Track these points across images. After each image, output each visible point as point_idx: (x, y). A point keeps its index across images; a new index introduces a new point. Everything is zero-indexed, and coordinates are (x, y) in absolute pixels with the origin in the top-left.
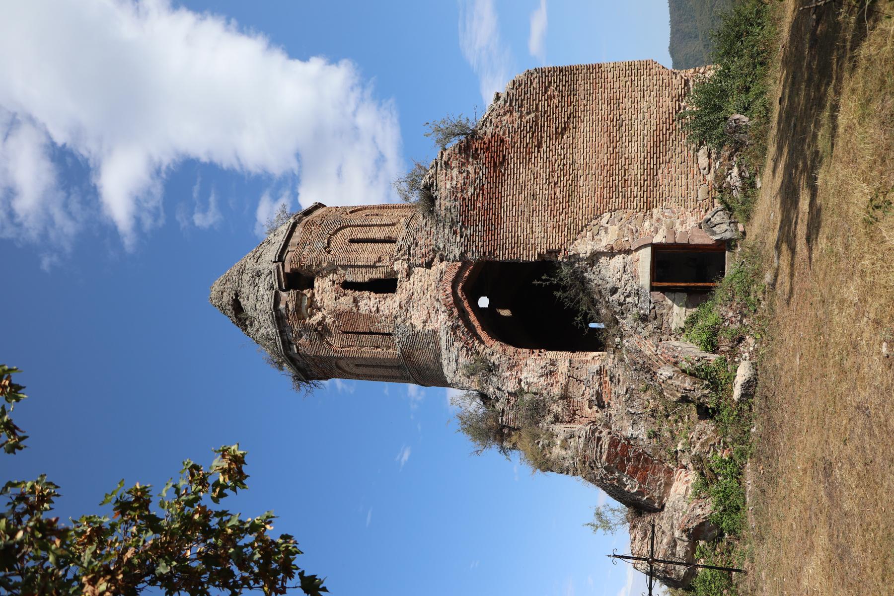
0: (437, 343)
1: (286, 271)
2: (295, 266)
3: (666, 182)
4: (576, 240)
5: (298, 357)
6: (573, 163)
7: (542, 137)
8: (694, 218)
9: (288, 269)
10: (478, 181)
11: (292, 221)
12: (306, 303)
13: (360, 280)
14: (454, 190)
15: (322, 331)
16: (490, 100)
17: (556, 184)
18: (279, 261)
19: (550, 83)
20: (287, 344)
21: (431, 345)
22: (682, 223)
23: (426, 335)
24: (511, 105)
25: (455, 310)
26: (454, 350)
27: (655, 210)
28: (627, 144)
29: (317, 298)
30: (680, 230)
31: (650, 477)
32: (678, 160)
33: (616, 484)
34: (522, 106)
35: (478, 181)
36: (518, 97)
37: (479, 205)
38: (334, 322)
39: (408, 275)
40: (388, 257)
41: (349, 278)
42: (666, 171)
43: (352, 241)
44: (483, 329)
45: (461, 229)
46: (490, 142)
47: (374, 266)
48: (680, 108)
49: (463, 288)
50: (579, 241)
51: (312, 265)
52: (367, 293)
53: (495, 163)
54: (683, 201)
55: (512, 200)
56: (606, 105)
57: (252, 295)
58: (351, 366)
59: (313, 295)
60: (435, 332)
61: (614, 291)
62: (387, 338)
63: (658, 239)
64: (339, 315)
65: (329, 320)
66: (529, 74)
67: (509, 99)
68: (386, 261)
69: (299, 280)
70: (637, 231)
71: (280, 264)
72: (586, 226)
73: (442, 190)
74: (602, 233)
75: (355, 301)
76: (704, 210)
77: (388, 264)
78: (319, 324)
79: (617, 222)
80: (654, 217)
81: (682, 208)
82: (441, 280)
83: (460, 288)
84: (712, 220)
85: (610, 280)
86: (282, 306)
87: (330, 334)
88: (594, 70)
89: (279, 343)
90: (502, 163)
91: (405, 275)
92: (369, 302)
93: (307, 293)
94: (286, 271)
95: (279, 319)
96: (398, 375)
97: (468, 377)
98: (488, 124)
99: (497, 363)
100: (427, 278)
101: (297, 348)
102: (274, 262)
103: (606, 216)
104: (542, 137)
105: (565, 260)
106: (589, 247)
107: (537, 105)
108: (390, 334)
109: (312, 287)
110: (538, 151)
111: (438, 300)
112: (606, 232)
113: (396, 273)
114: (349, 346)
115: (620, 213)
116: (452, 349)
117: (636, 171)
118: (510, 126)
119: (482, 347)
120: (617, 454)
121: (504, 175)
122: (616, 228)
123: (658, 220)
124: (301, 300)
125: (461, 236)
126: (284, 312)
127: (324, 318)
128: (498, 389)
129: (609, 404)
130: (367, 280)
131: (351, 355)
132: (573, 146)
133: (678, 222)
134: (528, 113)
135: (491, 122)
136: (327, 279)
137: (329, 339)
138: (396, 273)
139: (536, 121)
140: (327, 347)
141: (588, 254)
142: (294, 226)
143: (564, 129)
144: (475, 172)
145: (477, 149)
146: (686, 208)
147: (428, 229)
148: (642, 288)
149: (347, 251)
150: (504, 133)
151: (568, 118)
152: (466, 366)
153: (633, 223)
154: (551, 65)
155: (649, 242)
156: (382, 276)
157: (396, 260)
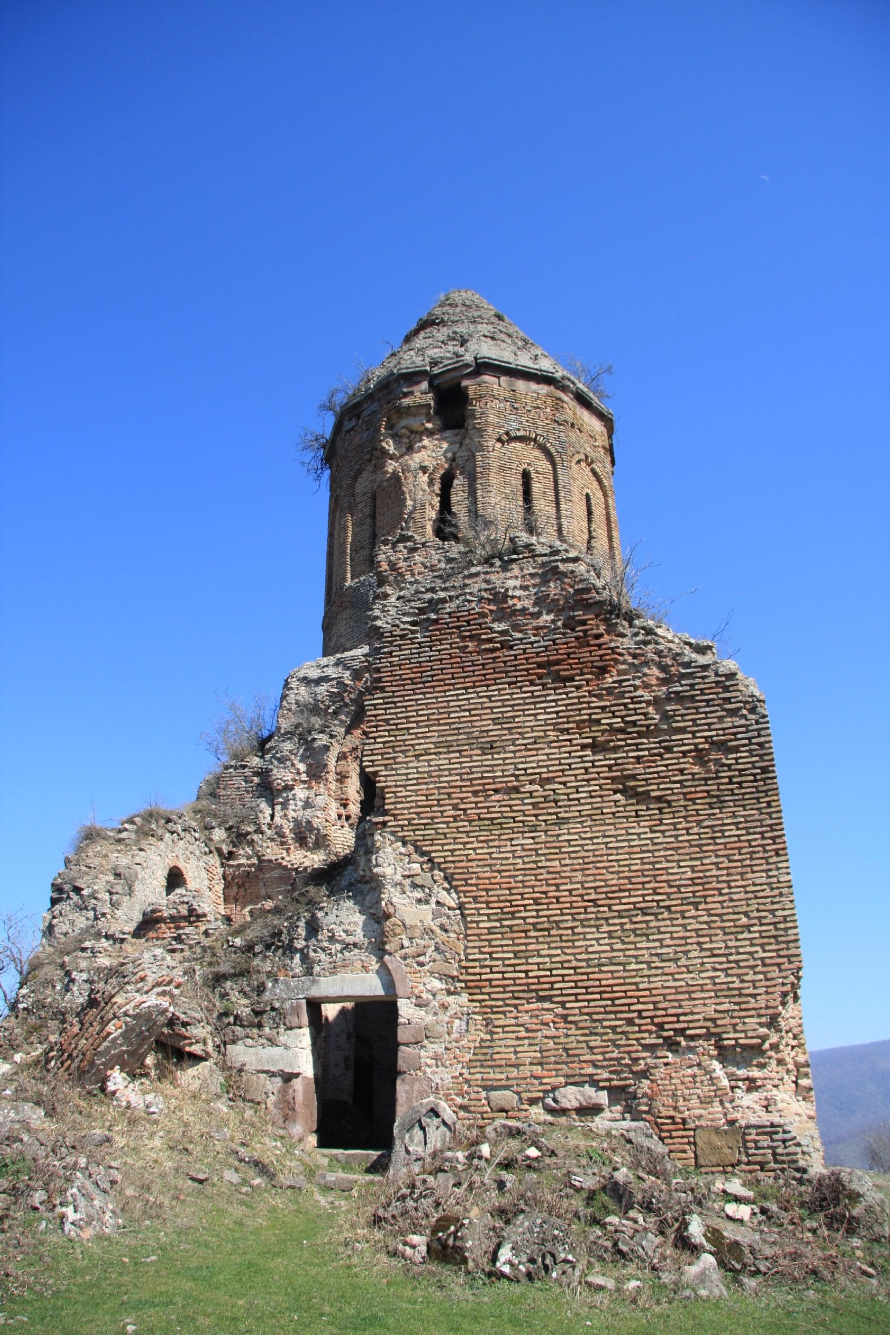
2: (471, 393)
3: (525, 1018)
4: (404, 844)
6: (561, 821)
8: (448, 1080)
9: (465, 383)
10: (519, 635)
14: (500, 598)
22: (437, 1058)
27: (464, 998)
28: (605, 928)
30: (423, 1053)
32: (572, 1042)
35: (519, 635)
36: (696, 690)
37: (471, 645)
42: (548, 1017)
43: (526, 477)
46: (599, 646)
48: (692, 1038)
50: (403, 850)
51: (476, 419)
53: (558, 662)
54: (484, 1056)
55: (478, 705)
56: (689, 875)
57: (430, 341)
61: (313, 928)
63: (406, 1009)
70: (421, 964)
73: (502, 575)
74: (418, 894)
76: (465, 1102)
79: (439, 921)
80: (451, 999)
81: (468, 1057)
84: (436, 1121)
85: (331, 918)
88: (775, 845)
98: (640, 638)
101: (352, 429)
102: (476, 359)
103: (451, 900)
104: (616, 749)
106: (389, 871)
107: (683, 730)
110: (584, 747)
112: (419, 901)
117: (544, 953)
118: (638, 682)
121: (532, 683)
122: (429, 921)
123: (444, 1007)
125: (413, 623)
132: (596, 817)
133: (439, 1048)
135: (646, 643)
141: (375, 870)
144: (537, 628)
145: (583, 623)
146: (470, 1065)
148: (314, 981)
149: (502, 468)
150: (620, 673)
151: (659, 799)
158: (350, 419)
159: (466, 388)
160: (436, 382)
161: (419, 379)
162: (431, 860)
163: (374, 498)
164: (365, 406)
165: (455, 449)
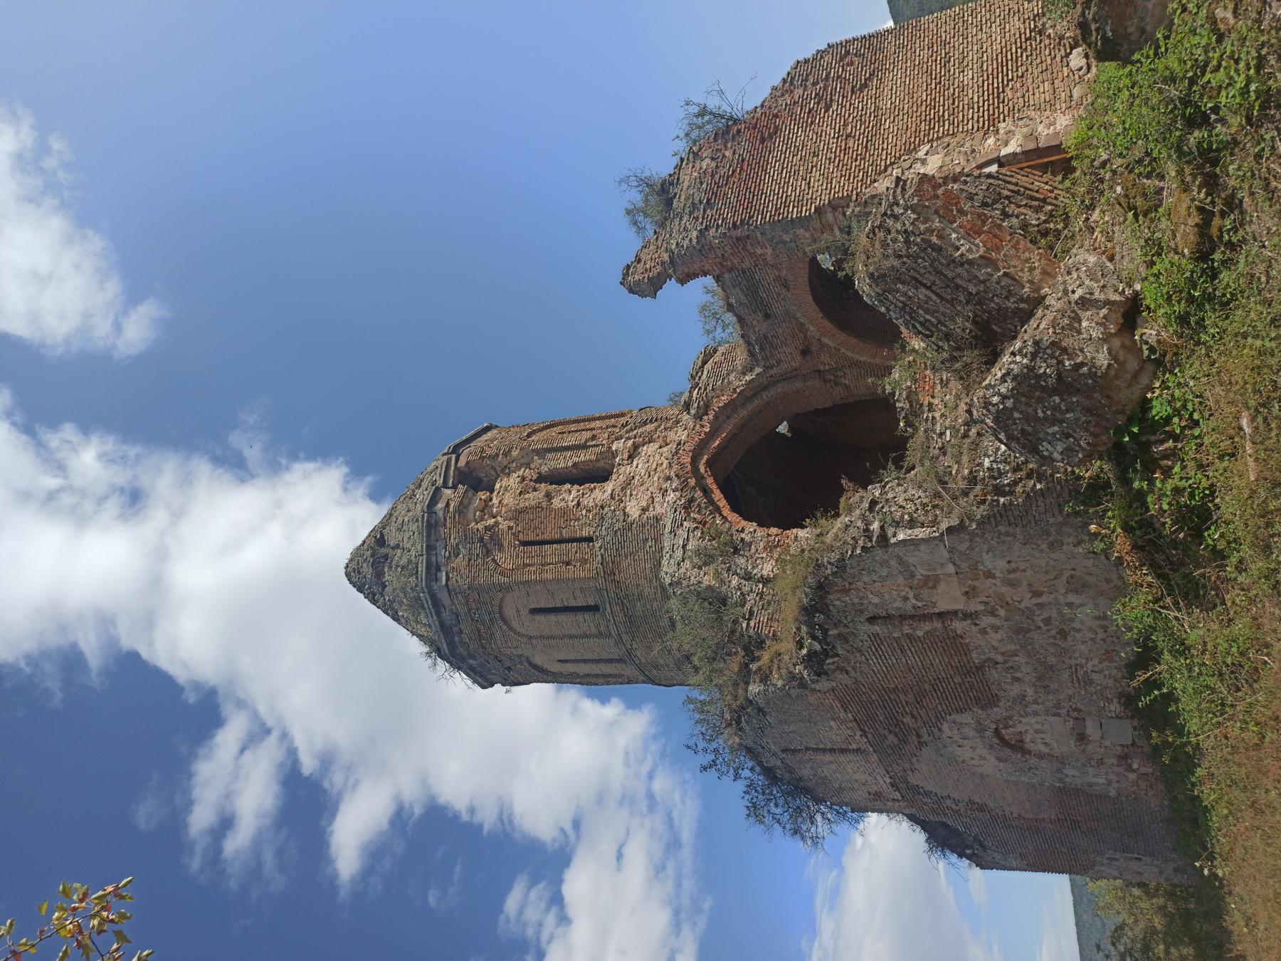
0: (658, 539)
3: (1019, 94)
5: (444, 597)
7: (831, 100)
9: (462, 463)
15: (490, 541)
16: (766, 93)
17: (848, 136)
18: (453, 452)
19: (848, 53)
20: (433, 569)
21: (650, 543)
23: (643, 526)
24: (791, 83)
25: (692, 482)
26: (682, 533)
27: (1002, 125)
29: (495, 501)
31: (1007, 249)
33: (934, 239)
34: (806, 80)
36: (802, 74)
38: (510, 528)
39: (631, 457)
41: (544, 469)
44: (735, 508)
45: (705, 211)
47: (584, 447)
49: (708, 463)
51: (497, 455)
52: (568, 486)
58: (524, 612)
59: (491, 500)
60: (657, 519)
62: (585, 545)
64: (518, 514)
65: (504, 525)
66: (821, 54)
67: (789, 80)
68: (603, 438)
69: (475, 480)
70: (974, 151)
72: (892, 164)
75: (548, 496)
78: (487, 528)
79: (940, 149)
80: (1001, 131)
82: (676, 453)
83: (703, 461)
86: (441, 505)
87: (501, 547)
89: (422, 569)
90: (770, 137)
91: (626, 456)
92: (568, 496)
93: (483, 495)
95: (431, 526)
96: (594, 631)
97: (700, 568)
99: (748, 538)
103: (926, 148)
104: (831, 100)
105: (858, 209)
107: (828, 76)
108: (589, 539)
109: (492, 491)
111: (668, 478)
113: (614, 455)
114: (525, 565)
115: (946, 140)
117: (972, 94)
119: (727, 525)
120: (936, 197)
124: (470, 500)
126: (441, 514)
127: (497, 524)
128: (748, 577)
129: (930, 404)
130: (570, 464)
131: (526, 578)
134: (814, 84)
137: (498, 556)
138: (614, 455)
139: (825, 88)
140: (492, 566)
143: (866, 85)
145: (739, 131)
147: (659, 243)
152: (698, 553)
153: (968, 145)
154: (849, 36)
155: (995, 155)
156: (594, 458)
157: (617, 439)
159: (468, 463)
160: (450, 484)
162: (892, 164)
164: (434, 559)
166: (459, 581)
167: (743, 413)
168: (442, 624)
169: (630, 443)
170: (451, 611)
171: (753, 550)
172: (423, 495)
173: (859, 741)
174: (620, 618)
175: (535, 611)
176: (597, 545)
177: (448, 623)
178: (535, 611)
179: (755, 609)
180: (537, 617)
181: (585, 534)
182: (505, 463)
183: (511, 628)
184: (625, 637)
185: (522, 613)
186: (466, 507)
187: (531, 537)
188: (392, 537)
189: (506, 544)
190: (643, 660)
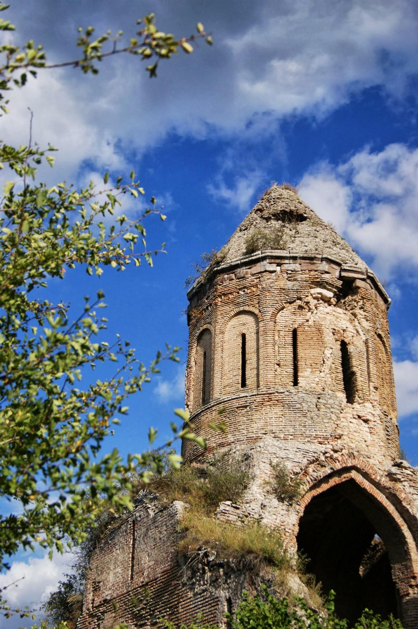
1: (357, 280)
9: (359, 283)
11: (389, 300)
12: (329, 294)
13: (354, 362)
21: (292, 430)
23: (305, 426)
40: (377, 398)
44: (314, 498)
59: (330, 305)
62: (292, 379)
71: (365, 277)
77: (371, 397)
78: (307, 303)
93: (333, 301)
94: (357, 280)
100: (357, 438)
108: (296, 383)
116: (299, 455)
130: (355, 369)
136: (348, 324)
142: (386, 301)
156: (359, 387)
158: (270, 263)
159: (359, 288)
160: (343, 274)
161: (334, 266)
163: (295, 333)
164: (287, 261)
165: (348, 326)
166: (267, 280)
167: (391, 509)
168: (237, 266)
169: (369, 417)
170: (247, 273)
171: (282, 512)
172: (334, 253)
173: (139, 580)
174: (236, 404)
175: (244, 336)
176: (293, 389)
177: (238, 270)
178: (244, 336)
179: (238, 511)
180: (240, 340)
181: (300, 380)
182: (359, 316)
183: (230, 319)
184: (221, 406)
185: (243, 327)
186: (325, 288)
187: (300, 338)
188: (303, 227)
189: (294, 317)
190: (203, 418)
